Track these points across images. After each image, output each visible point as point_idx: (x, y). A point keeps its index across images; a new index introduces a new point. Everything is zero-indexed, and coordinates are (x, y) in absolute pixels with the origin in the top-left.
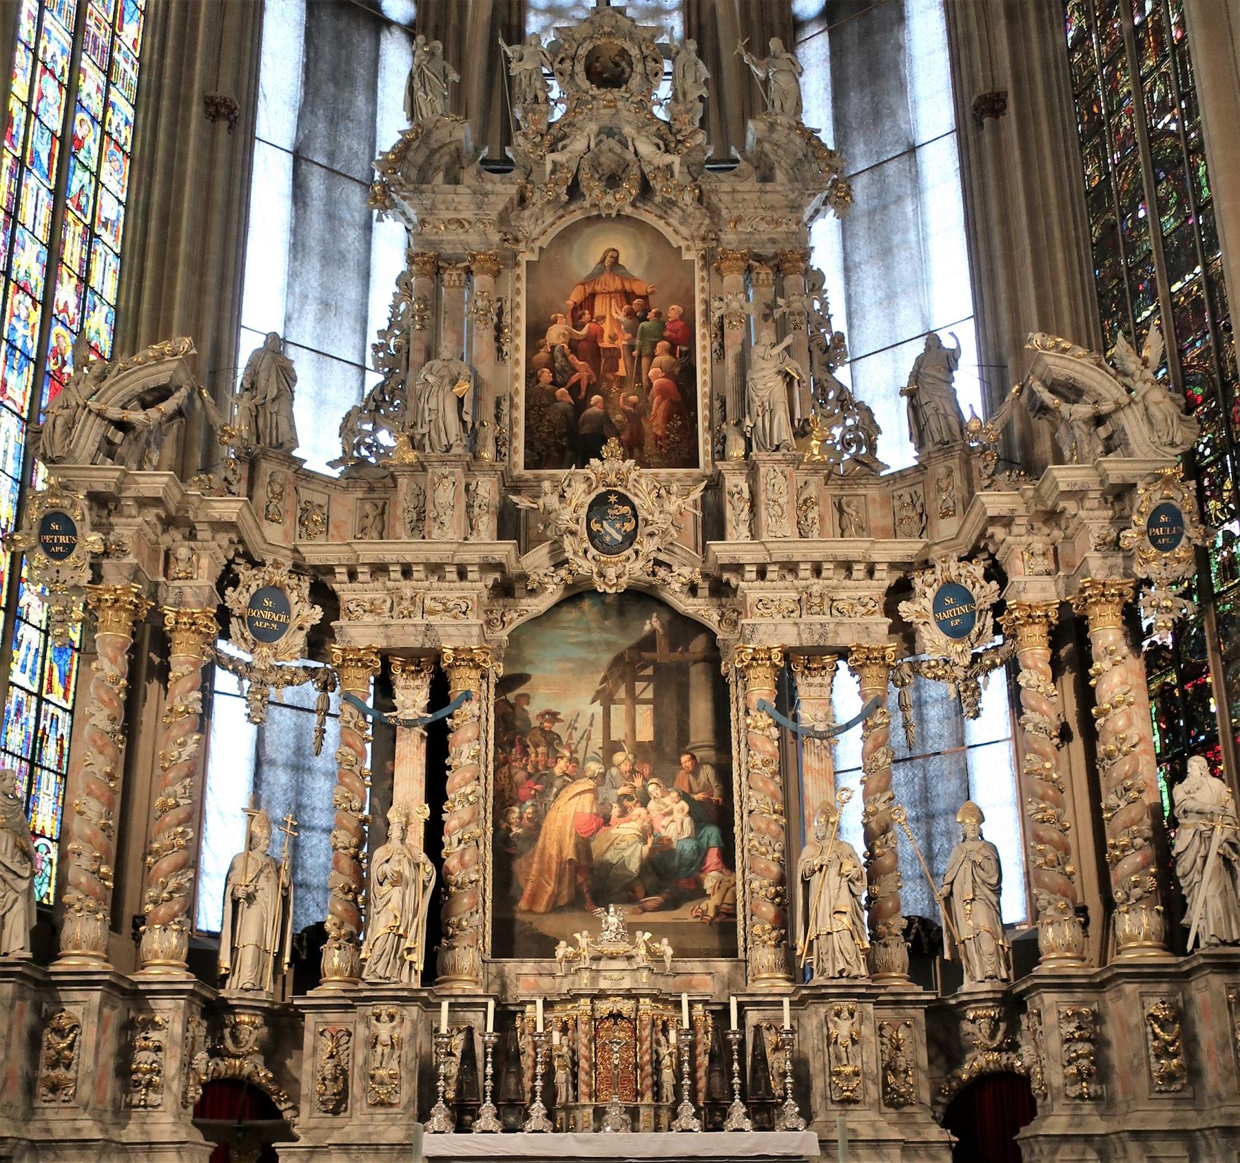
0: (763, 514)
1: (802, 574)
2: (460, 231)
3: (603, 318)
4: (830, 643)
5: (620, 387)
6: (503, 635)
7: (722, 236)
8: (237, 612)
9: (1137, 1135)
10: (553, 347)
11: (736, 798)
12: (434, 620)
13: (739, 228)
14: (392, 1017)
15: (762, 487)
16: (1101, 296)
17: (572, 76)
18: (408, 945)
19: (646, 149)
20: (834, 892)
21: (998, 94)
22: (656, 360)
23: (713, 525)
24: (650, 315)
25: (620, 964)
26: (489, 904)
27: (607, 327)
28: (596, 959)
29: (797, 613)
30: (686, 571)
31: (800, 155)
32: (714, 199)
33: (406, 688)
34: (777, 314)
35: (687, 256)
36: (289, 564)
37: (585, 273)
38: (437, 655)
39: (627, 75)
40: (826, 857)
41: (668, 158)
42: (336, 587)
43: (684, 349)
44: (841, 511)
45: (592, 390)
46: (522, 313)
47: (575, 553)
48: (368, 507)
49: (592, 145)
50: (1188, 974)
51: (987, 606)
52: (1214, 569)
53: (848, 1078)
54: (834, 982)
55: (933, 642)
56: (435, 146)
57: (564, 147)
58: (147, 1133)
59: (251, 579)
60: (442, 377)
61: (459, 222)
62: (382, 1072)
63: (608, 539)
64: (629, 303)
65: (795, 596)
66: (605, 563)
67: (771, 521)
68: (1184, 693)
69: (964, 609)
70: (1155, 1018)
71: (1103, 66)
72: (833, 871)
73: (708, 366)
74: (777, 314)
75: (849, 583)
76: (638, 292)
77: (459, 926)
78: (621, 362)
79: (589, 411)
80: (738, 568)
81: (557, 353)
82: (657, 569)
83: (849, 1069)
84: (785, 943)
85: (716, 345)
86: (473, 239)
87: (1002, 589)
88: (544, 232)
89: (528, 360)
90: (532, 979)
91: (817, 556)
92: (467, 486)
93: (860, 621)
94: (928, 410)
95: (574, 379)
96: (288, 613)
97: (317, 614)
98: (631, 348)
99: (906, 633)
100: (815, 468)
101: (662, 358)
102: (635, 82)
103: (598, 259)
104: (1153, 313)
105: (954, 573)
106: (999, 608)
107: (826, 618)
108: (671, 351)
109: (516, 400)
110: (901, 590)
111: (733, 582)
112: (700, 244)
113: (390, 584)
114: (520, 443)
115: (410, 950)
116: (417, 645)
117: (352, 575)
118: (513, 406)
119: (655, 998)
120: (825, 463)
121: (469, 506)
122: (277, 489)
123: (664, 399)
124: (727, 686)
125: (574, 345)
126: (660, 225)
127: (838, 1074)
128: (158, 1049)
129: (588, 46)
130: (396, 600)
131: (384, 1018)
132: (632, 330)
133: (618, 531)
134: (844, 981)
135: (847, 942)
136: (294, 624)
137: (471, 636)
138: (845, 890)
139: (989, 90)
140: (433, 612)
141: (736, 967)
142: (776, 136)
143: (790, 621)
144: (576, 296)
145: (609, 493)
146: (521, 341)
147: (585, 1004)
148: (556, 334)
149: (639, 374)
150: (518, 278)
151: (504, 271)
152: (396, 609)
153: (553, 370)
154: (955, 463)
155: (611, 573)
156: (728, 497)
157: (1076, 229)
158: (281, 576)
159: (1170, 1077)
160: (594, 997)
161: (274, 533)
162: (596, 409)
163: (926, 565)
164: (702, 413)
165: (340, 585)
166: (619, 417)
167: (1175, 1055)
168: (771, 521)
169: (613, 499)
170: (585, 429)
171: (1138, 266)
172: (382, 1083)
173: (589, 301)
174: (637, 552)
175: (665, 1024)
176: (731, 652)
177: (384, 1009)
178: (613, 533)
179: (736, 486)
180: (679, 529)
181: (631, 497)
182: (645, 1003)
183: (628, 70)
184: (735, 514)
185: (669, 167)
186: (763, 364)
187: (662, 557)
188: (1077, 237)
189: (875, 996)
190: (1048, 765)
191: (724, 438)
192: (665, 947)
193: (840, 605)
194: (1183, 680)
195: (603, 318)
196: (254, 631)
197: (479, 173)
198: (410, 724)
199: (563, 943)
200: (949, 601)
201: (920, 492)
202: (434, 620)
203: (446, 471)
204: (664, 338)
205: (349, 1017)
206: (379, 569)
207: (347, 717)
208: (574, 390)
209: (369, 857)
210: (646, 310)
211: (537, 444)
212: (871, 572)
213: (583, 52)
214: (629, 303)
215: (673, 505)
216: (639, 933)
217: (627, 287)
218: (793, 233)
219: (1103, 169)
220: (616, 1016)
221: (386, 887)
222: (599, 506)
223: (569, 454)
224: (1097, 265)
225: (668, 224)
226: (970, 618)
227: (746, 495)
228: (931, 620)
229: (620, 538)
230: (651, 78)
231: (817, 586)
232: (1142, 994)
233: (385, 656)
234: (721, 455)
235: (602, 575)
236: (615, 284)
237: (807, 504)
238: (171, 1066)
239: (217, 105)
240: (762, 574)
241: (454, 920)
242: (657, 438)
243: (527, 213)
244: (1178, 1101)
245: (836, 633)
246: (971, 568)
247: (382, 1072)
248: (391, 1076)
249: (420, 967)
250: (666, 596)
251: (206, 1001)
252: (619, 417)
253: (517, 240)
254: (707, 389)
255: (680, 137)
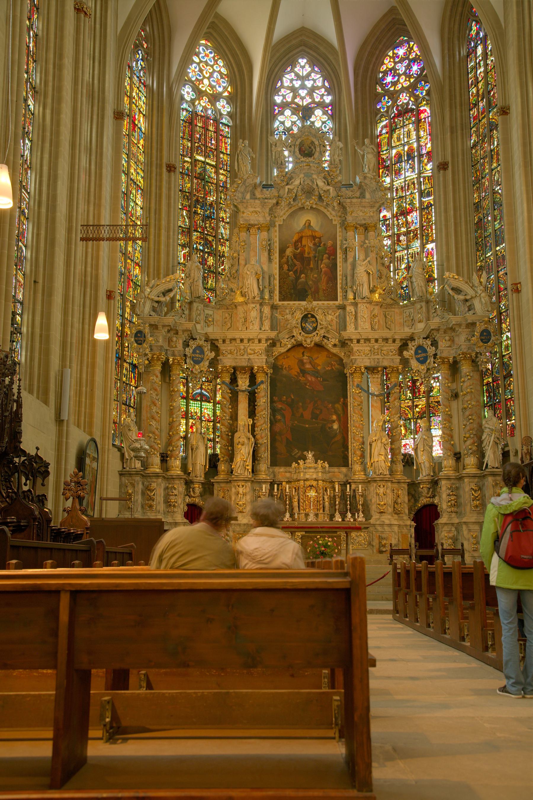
0: (359, 321)
1: (371, 342)
2: (256, 215)
3: (305, 246)
4: (380, 365)
5: (311, 271)
6: (272, 360)
7: (346, 217)
8: (189, 356)
9: (465, 523)
10: (288, 257)
11: (349, 415)
12: (251, 357)
13: (353, 215)
14: (243, 486)
15: (359, 311)
16: (476, 243)
17: (294, 152)
18: (247, 464)
19: (321, 183)
20: (379, 448)
21: (445, 163)
22: (324, 261)
23: (343, 326)
24: (321, 245)
25: (313, 470)
26: (269, 449)
27: (306, 249)
28: (305, 469)
29: (370, 355)
30: (333, 340)
31: (374, 188)
32: (344, 204)
33: (242, 378)
34: (365, 246)
35: (334, 223)
36: (204, 339)
37: (299, 229)
38: (252, 369)
39: (313, 152)
40: (377, 438)
41: (328, 187)
42: (218, 345)
43: (333, 257)
44: (386, 317)
45: (302, 272)
46: (277, 245)
47: (297, 334)
48: (227, 315)
49: (302, 182)
50: (484, 476)
51: (431, 355)
52: (503, 346)
53: (382, 506)
54: (379, 476)
55: (414, 364)
56: (247, 185)
57: (292, 183)
58: (175, 520)
59: (193, 344)
60: (252, 272)
61: (256, 212)
62: (241, 503)
63: (308, 329)
64: (314, 240)
65: (369, 348)
66: (307, 337)
67: (362, 323)
68: (493, 385)
69: (424, 355)
70: (473, 489)
71: (481, 159)
72: (379, 441)
73: (341, 264)
74: (365, 246)
75: (387, 344)
76: (317, 236)
77: (261, 457)
78: (311, 262)
79: (300, 280)
80: (351, 340)
81: (289, 259)
82: (324, 339)
83: (382, 503)
84: (363, 464)
85: (344, 256)
86: (261, 220)
87: (436, 350)
88: (284, 214)
89: (280, 261)
90: (283, 473)
91: (376, 337)
92: (261, 310)
93: (391, 358)
94: (415, 284)
95: (295, 268)
96: (204, 354)
97: (213, 355)
98: (315, 257)
99: (405, 362)
100: (377, 303)
101: (326, 261)
102: (316, 155)
103: (303, 224)
104: (491, 255)
105: (421, 343)
106: (435, 355)
107: (379, 357)
108: (329, 258)
109: (275, 276)
110: (404, 346)
111: (349, 344)
112: (339, 219)
113: (236, 344)
114: (277, 292)
115: (248, 465)
116: (246, 365)
117: (224, 341)
118: (274, 279)
119: (323, 481)
120: (380, 302)
121: (261, 318)
122: (199, 312)
123: (326, 275)
124: (347, 377)
125: (295, 256)
126: (325, 211)
127: (379, 504)
128: (176, 495)
129: (299, 141)
130: (238, 350)
131: (241, 486)
132: (315, 250)
133: (311, 326)
134: (382, 476)
135: (383, 464)
136: (206, 358)
137: (263, 362)
138: (383, 448)
139: (443, 161)
140: (250, 354)
141: (348, 470)
142: (366, 181)
143: (368, 358)
144: (296, 238)
145: (308, 314)
146: (277, 255)
147: (302, 483)
148: (289, 252)
149: (318, 267)
150: (276, 231)
151: (271, 228)
152: (238, 354)
153: (288, 265)
154: (423, 304)
155: (309, 341)
156: (347, 314)
157: (470, 217)
158: (202, 343)
159: (477, 506)
160: (304, 480)
161: (198, 326)
162: (303, 280)
163: (412, 339)
164: (339, 281)
165: (220, 344)
166: (311, 282)
167: (478, 500)
168: (362, 323)
169: (309, 316)
170: (299, 287)
171: (487, 236)
172: (240, 506)
173: (300, 239)
174: (317, 334)
175: (326, 488)
176: (348, 366)
177: (240, 483)
178: (309, 327)
179: (350, 310)
180: (331, 326)
181: (315, 315)
182: (320, 482)
183: (314, 150)
184: (350, 319)
185: (328, 190)
186: (361, 268)
187: (326, 335)
188: (470, 220)
189: (392, 481)
190: (447, 410)
191: (347, 291)
192: (326, 465)
193: (384, 352)
194: (493, 381)
195: (305, 246)
196: (194, 361)
197: (262, 191)
198: (243, 391)
199: (294, 463)
200: (420, 352)
201: (412, 312)
202: (251, 357)
203: (254, 305)
204: (326, 253)
205: (228, 485)
206: (233, 340)
207: (223, 389)
208: (295, 272)
209: (233, 436)
210: (320, 242)
211: (283, 292)
212: (394, 341)
213: (298, 143)
214: (314, 240)
215: (329, 318)
216: (319, 461)
217: (314, 234)
218: (372, 217)
219: (479, 196)
220: (311, 486)
221: (240, 446)
222: (305, 318)
223: (294, 295)
224: (476, 232)
225: (328, 211)
226: (426, 359)
227: (354, 313)
228: (414, 358)
229: (312, 329)
230: (322, 153)
231: (376, 346)
232: (469, 482)
233: (235, 368)
234: (345, 297)
235: (305, 341)
236: (310, 233)
237: (374, 316)
238: (180, 501)
239: (170, 167)
240: (358, 341)
241: (259, 455)
242: (324, 290)
243: (279, 207)
244: (478, 513)
245: (383, 362)
246: (427, 341)
247: (241, 503)
248: (243, 504)
249: (250, 470)
250: (326, 346)
251: (186, 480)
252: (311, 282)
253: (275, 217)
254: (341, 273)
255: (332, 177)
